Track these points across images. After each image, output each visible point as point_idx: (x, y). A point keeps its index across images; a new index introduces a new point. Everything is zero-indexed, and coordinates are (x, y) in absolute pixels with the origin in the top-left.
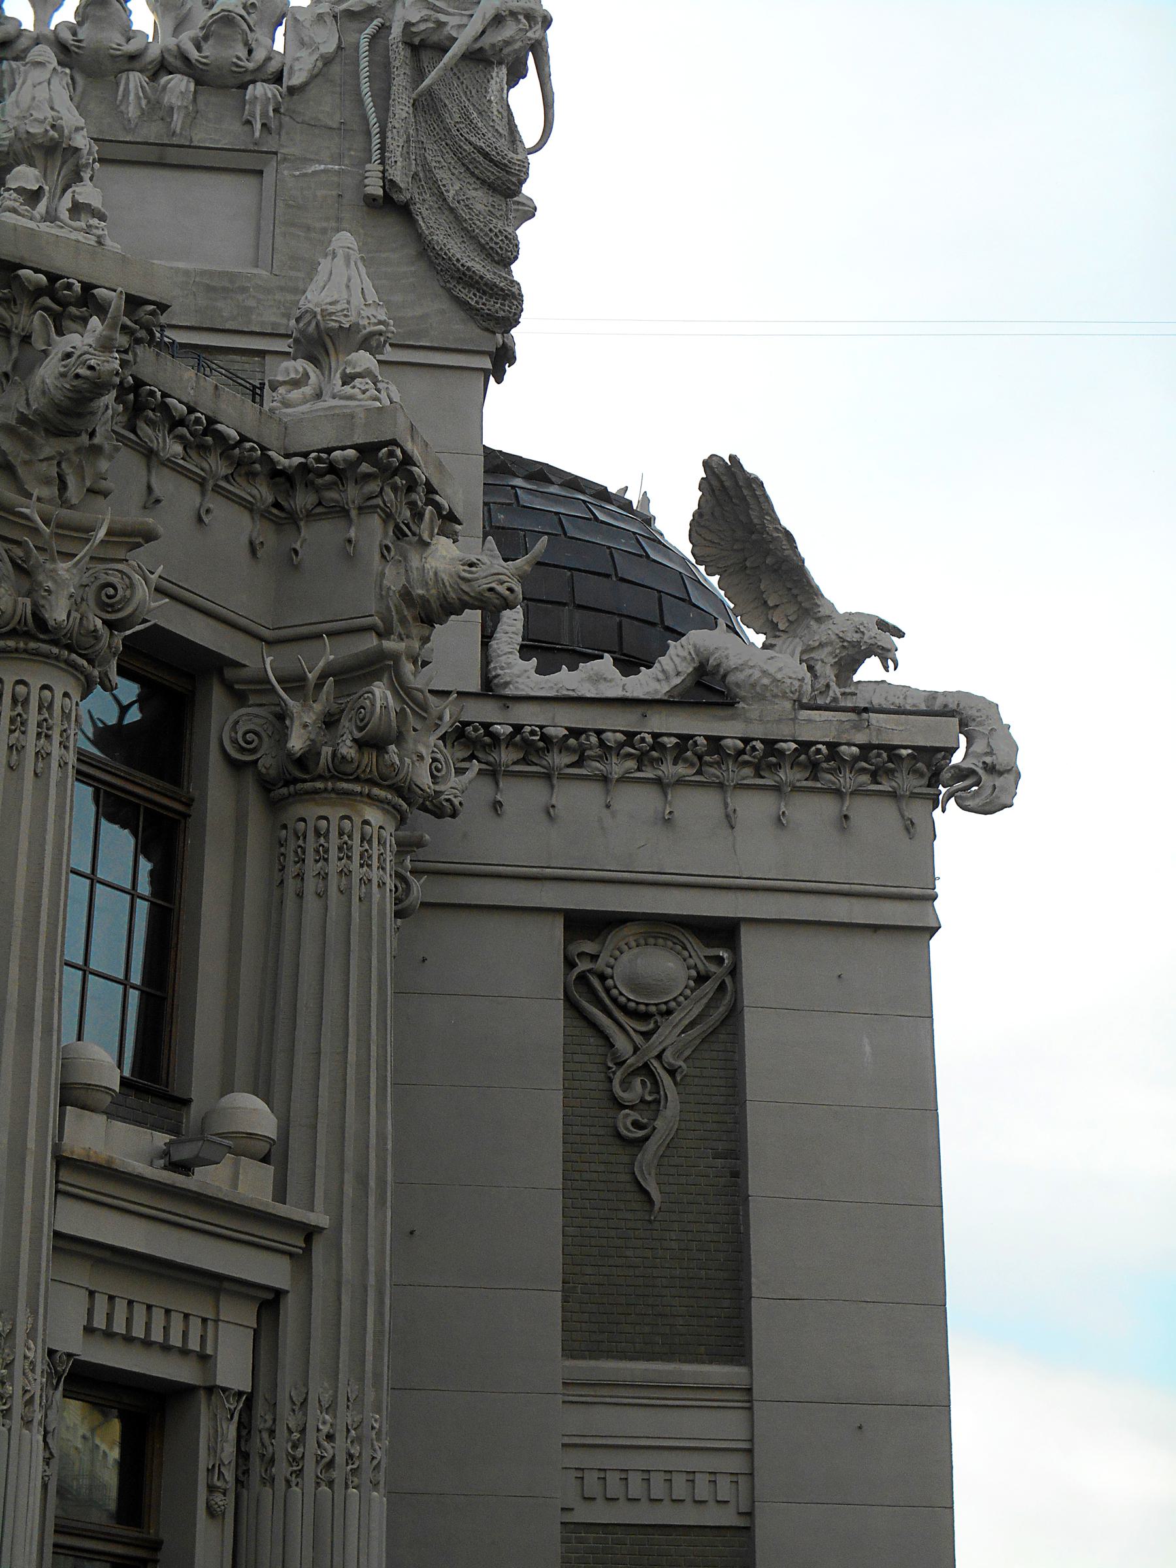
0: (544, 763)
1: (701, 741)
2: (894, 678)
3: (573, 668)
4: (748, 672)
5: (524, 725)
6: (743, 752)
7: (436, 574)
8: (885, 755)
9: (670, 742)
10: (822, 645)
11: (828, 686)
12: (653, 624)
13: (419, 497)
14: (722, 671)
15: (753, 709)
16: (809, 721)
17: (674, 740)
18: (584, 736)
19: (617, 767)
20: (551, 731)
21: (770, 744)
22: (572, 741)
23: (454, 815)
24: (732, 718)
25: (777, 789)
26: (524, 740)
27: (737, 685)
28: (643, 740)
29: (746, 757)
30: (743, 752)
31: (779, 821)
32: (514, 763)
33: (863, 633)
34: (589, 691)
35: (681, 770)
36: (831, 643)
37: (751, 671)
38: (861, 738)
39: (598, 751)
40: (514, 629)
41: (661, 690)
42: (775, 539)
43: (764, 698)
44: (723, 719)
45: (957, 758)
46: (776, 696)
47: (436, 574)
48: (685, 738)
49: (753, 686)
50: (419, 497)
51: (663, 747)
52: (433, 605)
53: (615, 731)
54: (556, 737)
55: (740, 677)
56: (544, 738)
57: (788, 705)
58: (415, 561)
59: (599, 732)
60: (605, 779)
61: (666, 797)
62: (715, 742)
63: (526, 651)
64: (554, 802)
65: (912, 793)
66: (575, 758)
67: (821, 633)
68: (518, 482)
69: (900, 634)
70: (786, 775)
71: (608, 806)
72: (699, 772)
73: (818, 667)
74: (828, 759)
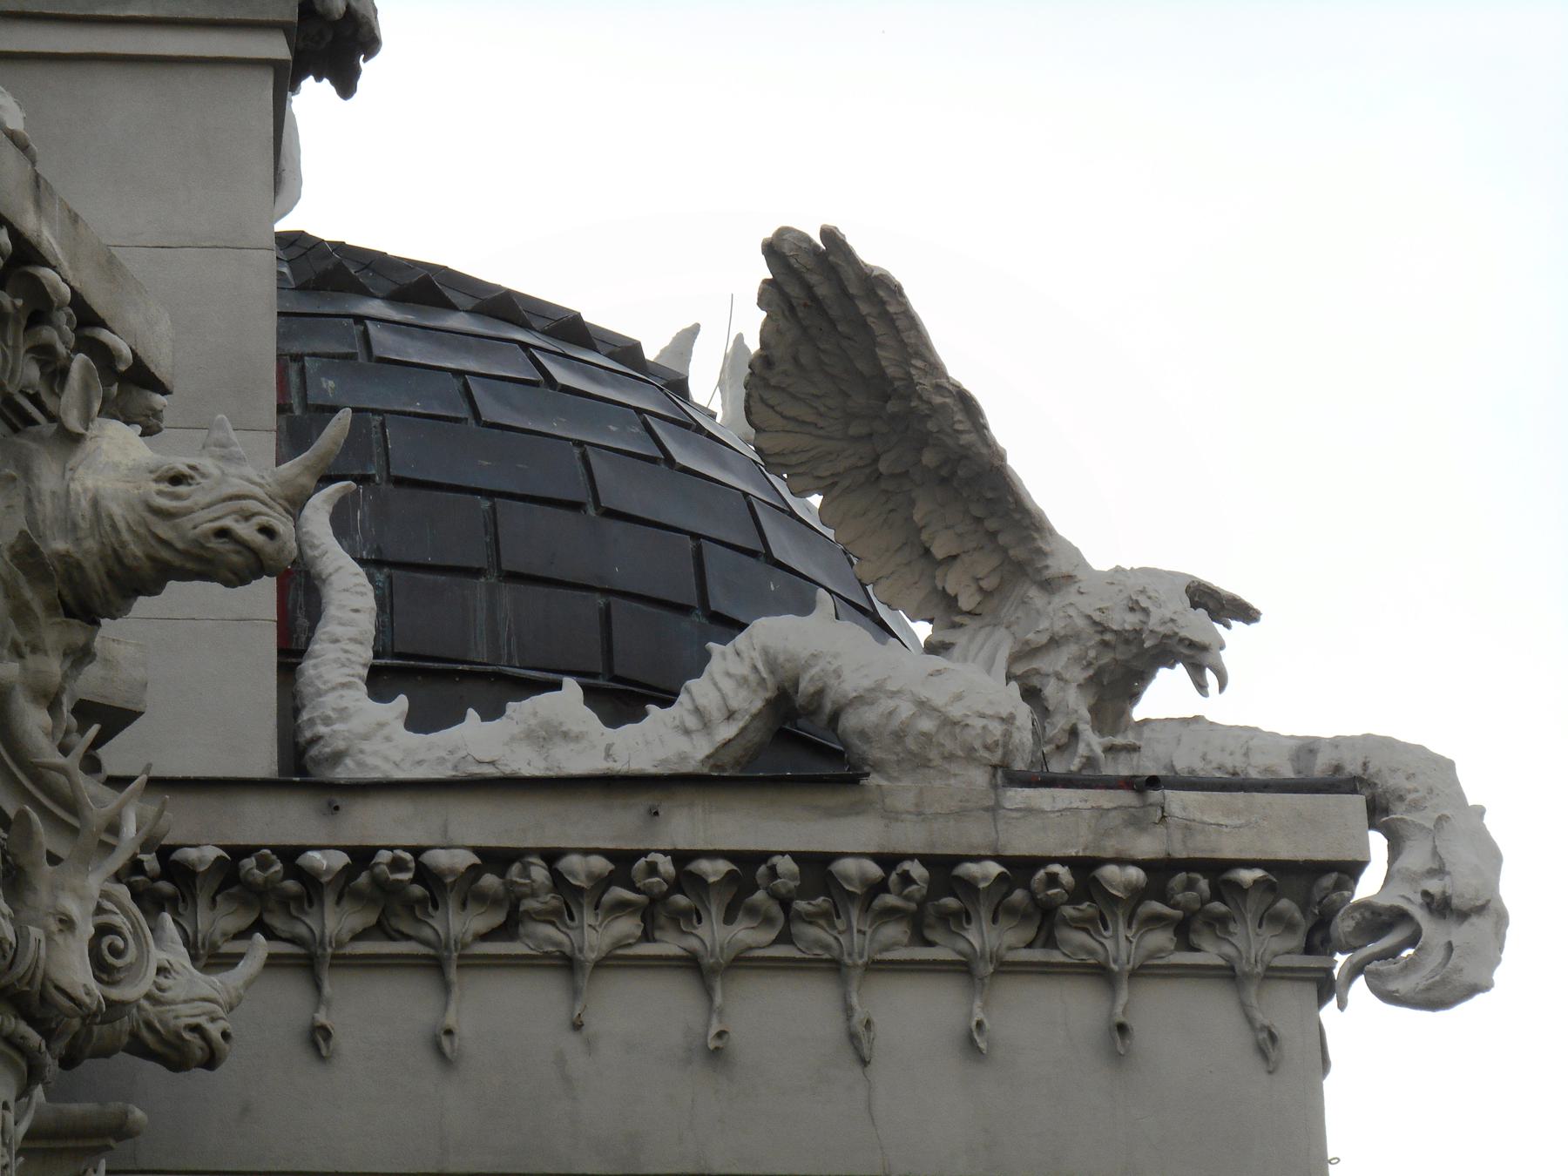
0: (427, 933)
1: (785, 865)
2: (1221, 709)
3: (492, 712)
4: (886, 704)
5: (373, 851)
6: (880, 887)
7: (95, 503)
8: (1203, 884)
9: (713, 870)
10: (1055, 642)
11: (1074, 733)
12: (684, 609)
13: (59, 334)
14: (828, 707)
15: (901, 790)
16: (1029, 811)
17: (723, 866)
18: (515, 868)
19: (596, 935)
20: (439, 859)
21: (942, 866)
22: (490, 881)
23: (211, 1060)
24: (855, 810)
25: (963, 968)
26: (378, 883)
27: (863, 735)
28: (652, 869)
29: (890, 900)
30: (880, 887)
31: (972, 1044)
32: (357, 937)
33: (1145, 611)
34: (528, 763)
35: (744, 933)
36: (1075, 636)
37: (891, 704)
38: (1148, 846)
39: (550, 900)
40: (352, 631)
41: (694, 753)
42: (935, 410)
43: (925, 763)
44: (830, 813)
45: (1369, 886)
46: (950, 757)
47: (95, 503)
48: (748, 862)
49: (899, 736)
50: (59, 334)
51: (697, 883)
52: (93, 576)
53: (587, 852)
54: (452, 871)
56: (425, 875)
57: (979, 777)
58: (48, 476)
59: (551, 857)
60: (566, 964)
61: (710, 998)
62: (817, 865)
63: (380, 681)
64: (450, 1020)
65: (1269, 968)
66: (498, 918)
67: (1051, 614)
68: (375, 307)
69: (1247, 614)
70: (983, 936)
71: (577, 1026)
72: (785, 938)
73: (1050, 690)
74: (1074, 897)
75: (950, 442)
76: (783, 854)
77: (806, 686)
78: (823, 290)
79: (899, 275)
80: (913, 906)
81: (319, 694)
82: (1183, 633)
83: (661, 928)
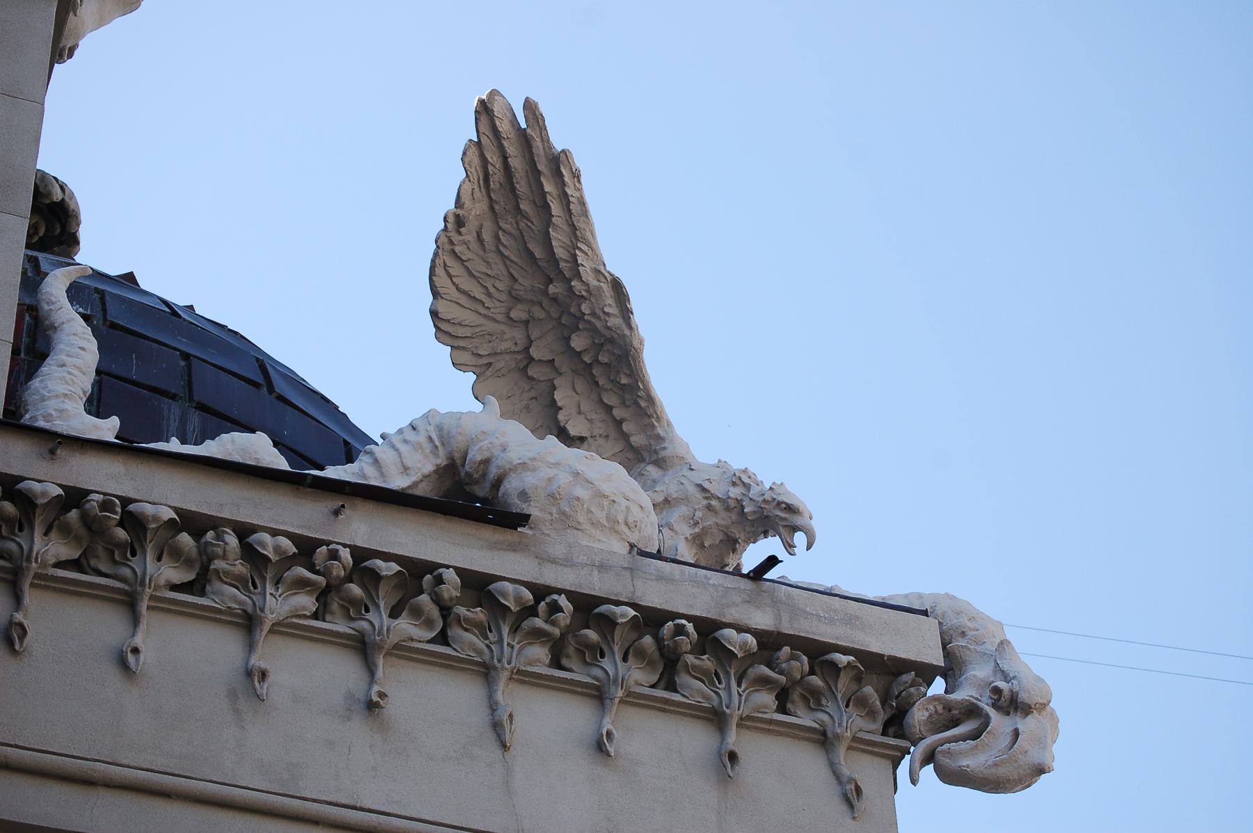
0: (126, 572)
1: (449, 575)
4: (546, 472)
9: (389, 569)
14: (493, 472)
16: (661, 578)
17: (395, 567)
21: (586, 605)
22: (185, 539)
24: (512, 548)
26: (86, 519)
28: (334, 555)
29: (539, 622)
30: (531, 611)
32: (59, 565)
35: (405, 626)
36: (685, 500)
37: (550, 472)
38: (763, 620)
39: (240, 568)
44: (494, 546)
51: (373, 578)
53: (275, 533)
54: (156, 518)
55: (530, 480)
59: (244, 531)
72: (442, 638)
74: (699, 650)
75: (599, 325)
76: (448, 567)
77: (475, 455)
78: (516, 163)
79: (579, 161)
80: (557, 632)
81: (43, 399)
82: (780, 498)
83: (332, 613)
